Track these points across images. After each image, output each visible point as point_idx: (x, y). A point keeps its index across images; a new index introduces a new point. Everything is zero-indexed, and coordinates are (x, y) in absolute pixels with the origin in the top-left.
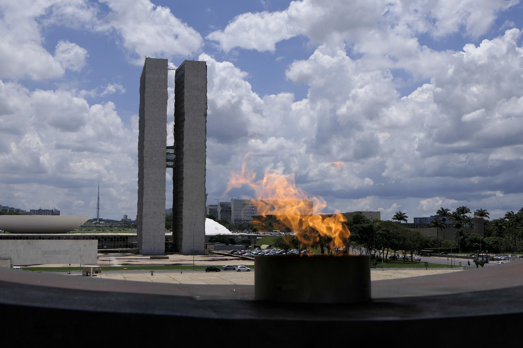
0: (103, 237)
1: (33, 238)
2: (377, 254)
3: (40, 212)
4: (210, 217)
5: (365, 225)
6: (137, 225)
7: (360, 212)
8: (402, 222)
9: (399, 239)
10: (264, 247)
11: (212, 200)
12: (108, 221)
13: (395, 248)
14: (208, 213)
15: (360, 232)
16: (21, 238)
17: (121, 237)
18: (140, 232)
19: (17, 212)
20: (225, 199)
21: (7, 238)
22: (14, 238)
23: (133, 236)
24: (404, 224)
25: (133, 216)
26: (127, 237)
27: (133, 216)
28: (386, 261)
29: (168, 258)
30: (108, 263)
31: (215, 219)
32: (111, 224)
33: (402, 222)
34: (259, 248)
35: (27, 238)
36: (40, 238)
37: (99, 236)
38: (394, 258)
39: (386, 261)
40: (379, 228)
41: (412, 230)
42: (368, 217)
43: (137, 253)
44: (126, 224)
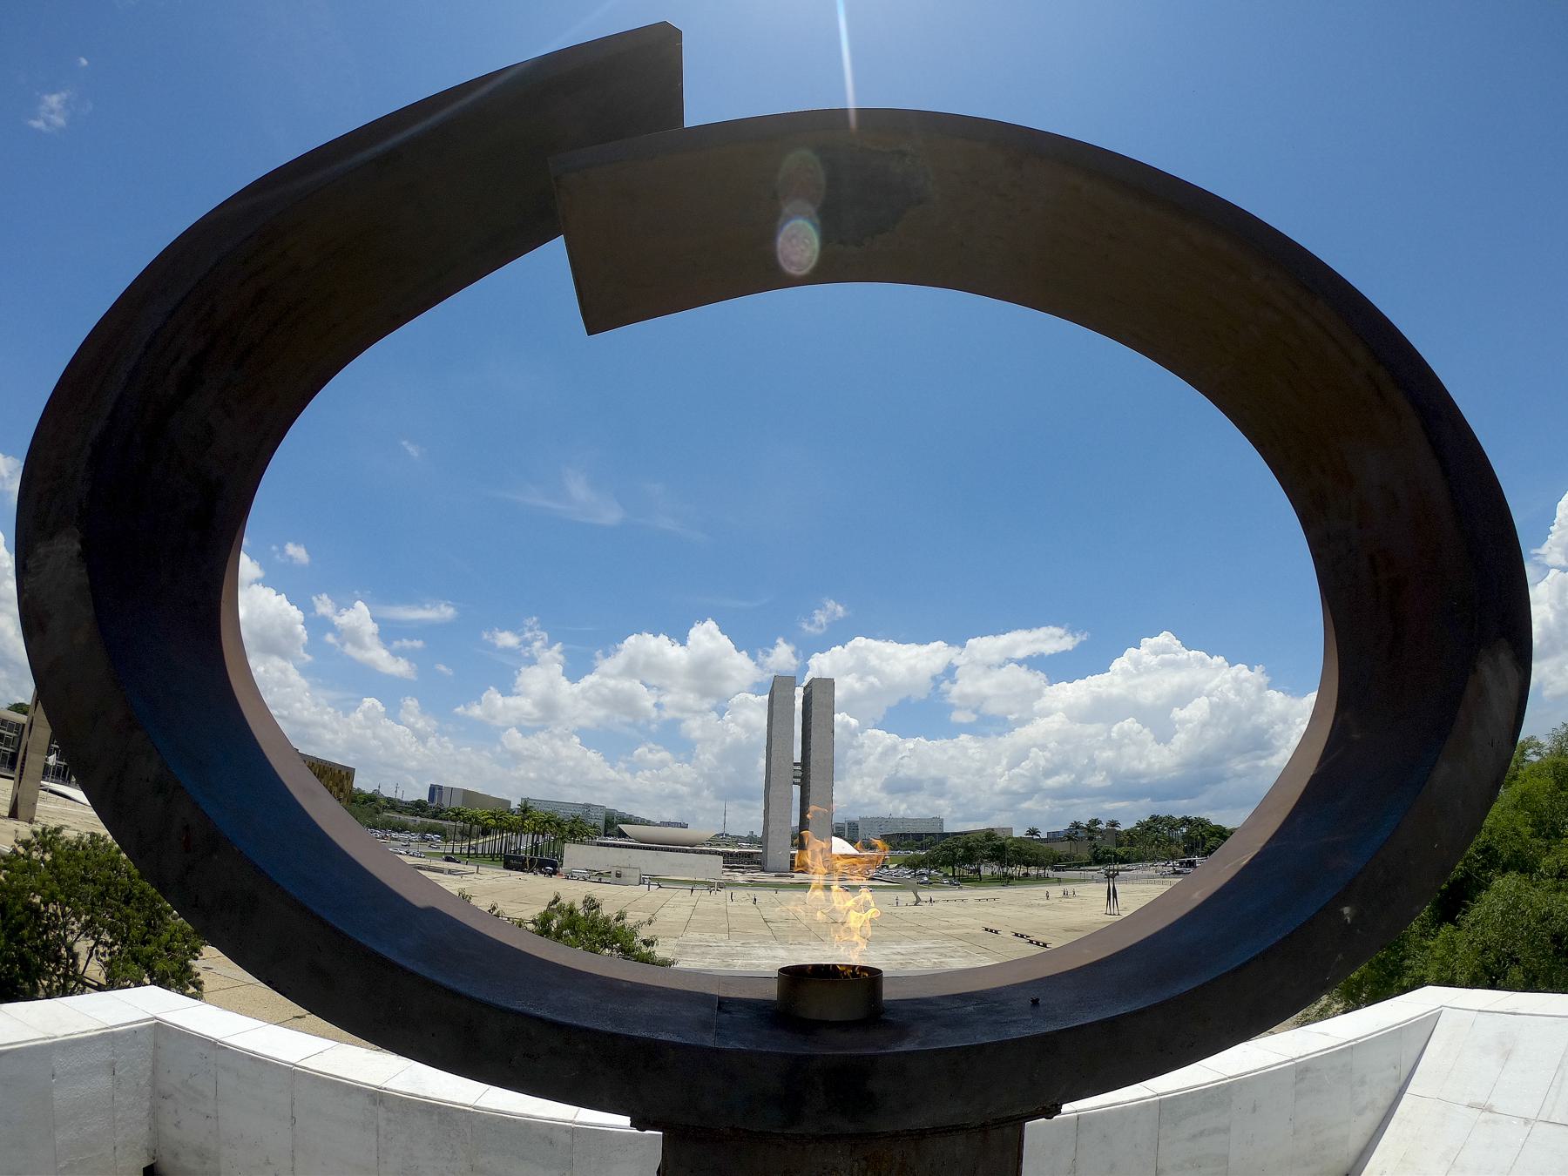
0: (728, 853)
1: (662, 849)
2: (1010, 871)
3: (669, 824)
4: (838, 835)
5: (998, 843)
6: (762, 842)
7: (993, 829)
8: (1035, 837)
9: (1031, 856)
10: (891, 866)
11: (839, 818)
12: (734, 837)
13: (1028, 865)
14: (835, 832)
15: (992, 849)
16: (650, 849)
17: (746, 853)
18: (765, 848)
19: (648, 823)
20: (855, 817)
21: (638, 848)
22: (644, 848)
23: (758, 853)
24: (1037, 839)
25: (759, 833)
26: (752, 853)
27: (759, 833)
28: (1019, 878)
29: (793, 877)
30: (729, 877)
31: (841, 837)
32: (737, 840)
33: (1035, 837)
34: (888, 867)
35: (656, 849)
36: (668, 850)
37: (725, 852)
38: (1027, 875)
39: (1019, 878)
40: (1012, 844)
41: (1044, 845)
42: (1000, 834)
43: (763, 870)
44: (751, 840)
